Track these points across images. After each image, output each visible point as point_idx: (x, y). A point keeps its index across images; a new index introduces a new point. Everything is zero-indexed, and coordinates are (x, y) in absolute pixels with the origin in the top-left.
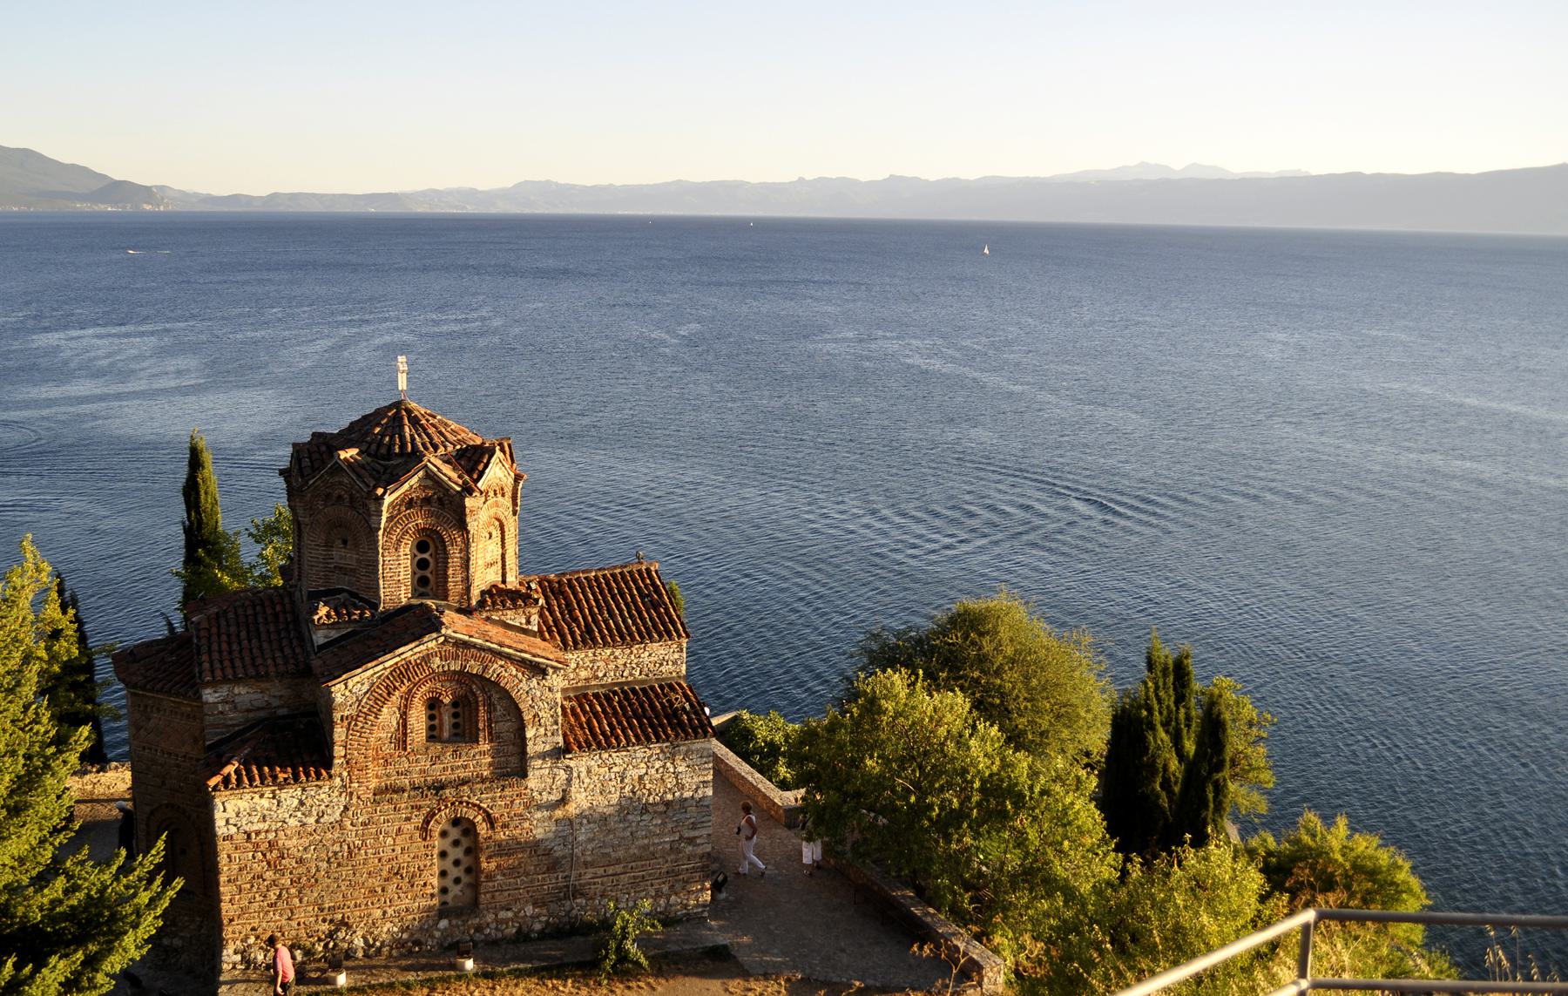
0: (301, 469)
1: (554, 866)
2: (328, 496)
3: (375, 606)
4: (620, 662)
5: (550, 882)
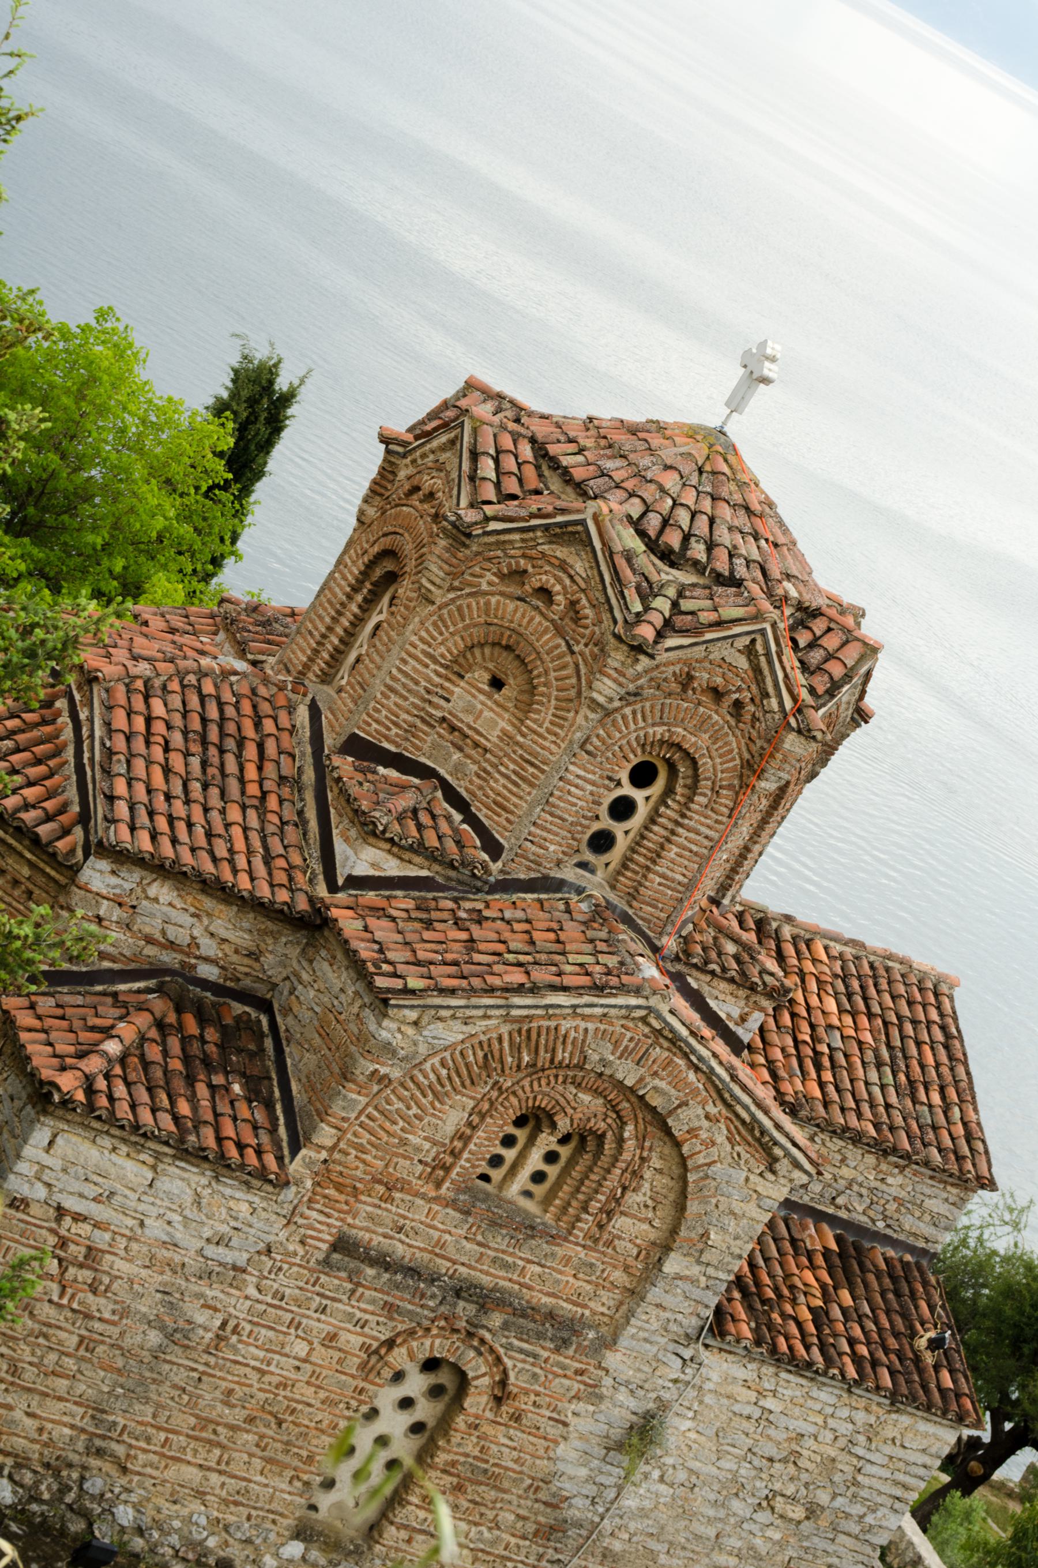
2: (519, 575)
3: (494, 849)
4: (846, 1172)
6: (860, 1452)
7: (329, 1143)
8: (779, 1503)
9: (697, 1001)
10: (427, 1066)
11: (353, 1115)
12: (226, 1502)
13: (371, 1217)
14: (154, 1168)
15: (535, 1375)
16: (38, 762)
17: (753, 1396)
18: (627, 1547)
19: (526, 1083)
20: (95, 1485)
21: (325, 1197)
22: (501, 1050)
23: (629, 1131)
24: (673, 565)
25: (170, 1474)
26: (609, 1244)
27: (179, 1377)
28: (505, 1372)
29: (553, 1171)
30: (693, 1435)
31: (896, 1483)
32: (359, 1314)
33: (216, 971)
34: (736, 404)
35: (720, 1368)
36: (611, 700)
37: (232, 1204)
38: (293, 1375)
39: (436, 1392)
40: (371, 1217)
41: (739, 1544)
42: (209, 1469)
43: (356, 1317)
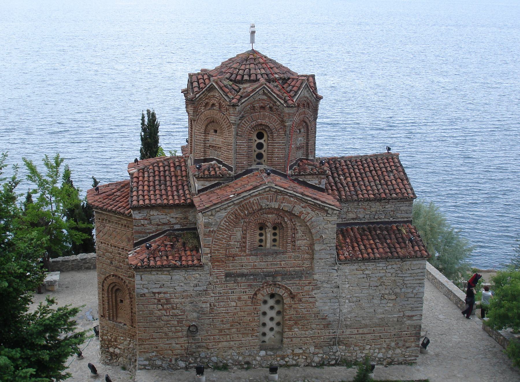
0: (192, 88)
1: (327, 326)
3: (230, 169)
5: (326, 334)
6: (401, 275)
7: (209, 252)
8: (386, 296)
9: (305, 184)
10: (222, 224)
11: (211, 243)
12: (239, 348)
13: (233, 266)
14: (169, 274)
15: (298, 288)
16: (124, 197)
17: (361, 272)
18: (351, 322)
19: (252, 218)
20: (203, 355)
21: (216, 265)
22: (238, 213)
23: (286, 218)
24: (242, 84)
25: (220, 346)
26: (299, 249)
27: (207, 321)
28: (290, 290)
29: (277, 237)
30: (351, 288)
31: (416, 279)
32: (243, 290)
33: (179, 226)
34: (252, 41)
35: (347, 269)
36: (235, 121)
37: (193, 275)
38: (235, 311)
39: (278, 302)
40: (233, 266)
41: (382, 311)
42: (229, 341)
43: (242, 291)
